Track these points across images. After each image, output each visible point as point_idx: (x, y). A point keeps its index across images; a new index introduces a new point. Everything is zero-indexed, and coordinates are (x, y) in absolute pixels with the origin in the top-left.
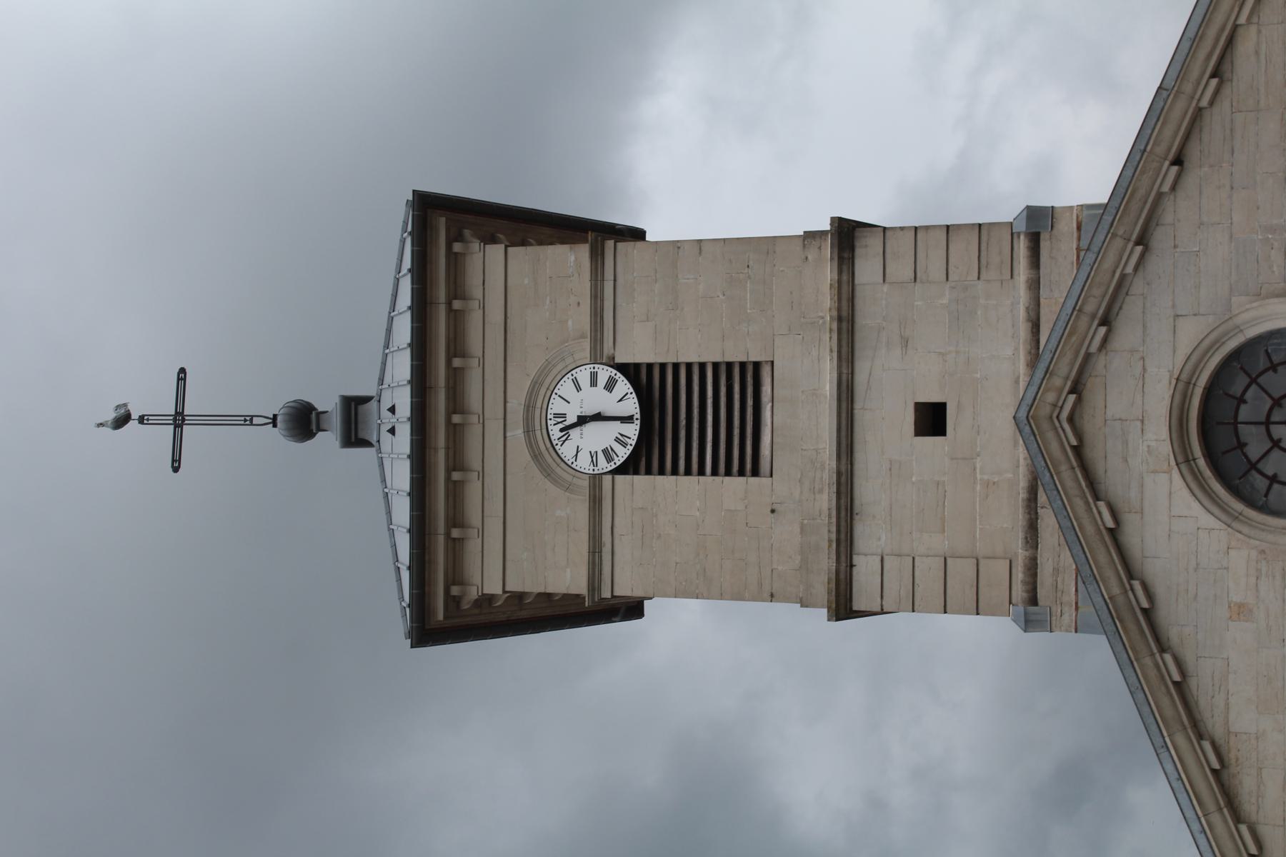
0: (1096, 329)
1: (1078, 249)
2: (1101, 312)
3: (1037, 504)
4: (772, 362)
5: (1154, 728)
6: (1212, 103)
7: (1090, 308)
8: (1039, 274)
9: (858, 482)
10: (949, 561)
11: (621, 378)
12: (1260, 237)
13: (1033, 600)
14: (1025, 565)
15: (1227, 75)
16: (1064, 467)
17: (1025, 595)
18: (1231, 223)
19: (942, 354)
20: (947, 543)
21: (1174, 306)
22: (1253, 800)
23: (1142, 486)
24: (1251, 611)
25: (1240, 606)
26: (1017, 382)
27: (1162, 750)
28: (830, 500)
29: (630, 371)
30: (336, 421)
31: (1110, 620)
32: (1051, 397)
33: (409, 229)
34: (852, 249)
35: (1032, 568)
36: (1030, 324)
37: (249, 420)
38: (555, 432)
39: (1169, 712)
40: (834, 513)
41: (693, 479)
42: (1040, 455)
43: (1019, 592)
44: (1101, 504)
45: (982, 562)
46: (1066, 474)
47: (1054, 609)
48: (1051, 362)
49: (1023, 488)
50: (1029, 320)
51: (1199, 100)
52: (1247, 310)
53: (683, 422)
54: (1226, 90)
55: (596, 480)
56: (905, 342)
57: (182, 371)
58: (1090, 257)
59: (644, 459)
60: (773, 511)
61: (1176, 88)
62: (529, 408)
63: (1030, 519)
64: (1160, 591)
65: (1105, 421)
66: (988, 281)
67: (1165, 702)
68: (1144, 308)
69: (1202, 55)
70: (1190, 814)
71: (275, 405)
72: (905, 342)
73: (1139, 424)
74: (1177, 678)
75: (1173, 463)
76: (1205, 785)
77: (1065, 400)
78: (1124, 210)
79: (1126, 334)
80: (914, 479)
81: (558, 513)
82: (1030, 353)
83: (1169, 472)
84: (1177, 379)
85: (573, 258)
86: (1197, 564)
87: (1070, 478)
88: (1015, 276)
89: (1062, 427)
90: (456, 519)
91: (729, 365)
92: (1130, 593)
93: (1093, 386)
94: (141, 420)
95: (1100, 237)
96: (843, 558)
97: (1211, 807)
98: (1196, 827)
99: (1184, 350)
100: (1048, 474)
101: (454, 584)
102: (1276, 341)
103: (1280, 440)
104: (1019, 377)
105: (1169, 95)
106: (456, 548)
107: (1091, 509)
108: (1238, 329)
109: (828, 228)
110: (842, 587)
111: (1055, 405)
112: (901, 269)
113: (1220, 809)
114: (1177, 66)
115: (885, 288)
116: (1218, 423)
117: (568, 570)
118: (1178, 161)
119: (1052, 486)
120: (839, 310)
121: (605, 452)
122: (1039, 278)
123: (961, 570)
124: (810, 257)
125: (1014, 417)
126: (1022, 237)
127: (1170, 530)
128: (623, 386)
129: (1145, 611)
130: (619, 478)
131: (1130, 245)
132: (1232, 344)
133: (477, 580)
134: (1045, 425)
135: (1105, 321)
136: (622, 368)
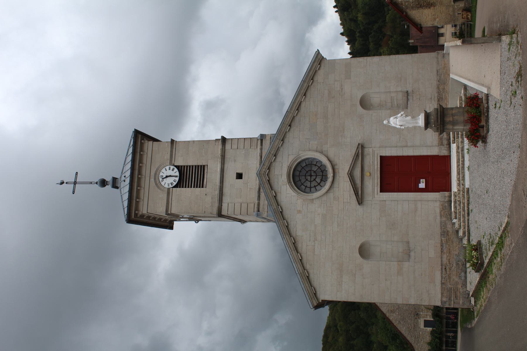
1: (270, 142)
2: (274, 153)
4: (207, 165)
6: (296, 115)
7: (272, 153)
9: (224, 188)
10: (242, 204)
11: (175, 168)
13: (259, 211)
16: (266, 184)
17: (257, 210)
19: (242, 163)
21: (288, 153)
22: (301, 249)
26: (257, 168)
28: (218, 192)
29: (177, 167)
30: (111, 183)
32: (264, 170)
33: (133, 137)
34: (225, 142)
35: (259, 205)
37: (91, 183)
38: (161, 179)
39: (285, 231)
40: (219, 194)
41: (190, 188)
43: (256, 209)
46: (266, 185)
50: (260, 156)
51: (294, 114)
53: (188, 177)
54: (299, 113)
55: (169, 189)
56: (235, 161)
57: (77, 173)
58: (273, 143)
59: (179, 185)
60: (206, 195)
62: (155, 174)
63: (259, 195)
66: (252, 149)
67: (284, 229)
69: (295, 106)
70: (288, 251)
71: (97, 180)
72: (235, 161)
73: (281, 176)
74: (287, 225)
75: (287, 182)
76: (292, 246)
79: (279, 159)
80: (235, 188)
81: (160, 196)
83: (286, 185)
85: (167, 144)
87: (267, 186)
90: (138, 197)
91: (198, 166)
93: (272, 168)
94: (67, 183)
95: (275, 139)
96: (220, 204)
97: (293, 250)
98: (289, 253)
99: (290, 160)
101: (136, 211)
103: (307, 179)
106: (137, 203)
107: (271, 192)
109: (220, 138)
110: (220, 209)
111: (265, 172)
112: (234, 146)
113: (294, 250)
114: (290, 107)
115: (231, 150)
117: (161, 208)
118: (290, 126)
120: (222, 154)
121: (171, 183)
123: (244, 206)
124: (216, 144)
128: (176, 170)
130: (173, 188)
131: (280, 141)
132: (299, 160)
133: (141, 210)
135: (275, 156)
136: (176, 166)
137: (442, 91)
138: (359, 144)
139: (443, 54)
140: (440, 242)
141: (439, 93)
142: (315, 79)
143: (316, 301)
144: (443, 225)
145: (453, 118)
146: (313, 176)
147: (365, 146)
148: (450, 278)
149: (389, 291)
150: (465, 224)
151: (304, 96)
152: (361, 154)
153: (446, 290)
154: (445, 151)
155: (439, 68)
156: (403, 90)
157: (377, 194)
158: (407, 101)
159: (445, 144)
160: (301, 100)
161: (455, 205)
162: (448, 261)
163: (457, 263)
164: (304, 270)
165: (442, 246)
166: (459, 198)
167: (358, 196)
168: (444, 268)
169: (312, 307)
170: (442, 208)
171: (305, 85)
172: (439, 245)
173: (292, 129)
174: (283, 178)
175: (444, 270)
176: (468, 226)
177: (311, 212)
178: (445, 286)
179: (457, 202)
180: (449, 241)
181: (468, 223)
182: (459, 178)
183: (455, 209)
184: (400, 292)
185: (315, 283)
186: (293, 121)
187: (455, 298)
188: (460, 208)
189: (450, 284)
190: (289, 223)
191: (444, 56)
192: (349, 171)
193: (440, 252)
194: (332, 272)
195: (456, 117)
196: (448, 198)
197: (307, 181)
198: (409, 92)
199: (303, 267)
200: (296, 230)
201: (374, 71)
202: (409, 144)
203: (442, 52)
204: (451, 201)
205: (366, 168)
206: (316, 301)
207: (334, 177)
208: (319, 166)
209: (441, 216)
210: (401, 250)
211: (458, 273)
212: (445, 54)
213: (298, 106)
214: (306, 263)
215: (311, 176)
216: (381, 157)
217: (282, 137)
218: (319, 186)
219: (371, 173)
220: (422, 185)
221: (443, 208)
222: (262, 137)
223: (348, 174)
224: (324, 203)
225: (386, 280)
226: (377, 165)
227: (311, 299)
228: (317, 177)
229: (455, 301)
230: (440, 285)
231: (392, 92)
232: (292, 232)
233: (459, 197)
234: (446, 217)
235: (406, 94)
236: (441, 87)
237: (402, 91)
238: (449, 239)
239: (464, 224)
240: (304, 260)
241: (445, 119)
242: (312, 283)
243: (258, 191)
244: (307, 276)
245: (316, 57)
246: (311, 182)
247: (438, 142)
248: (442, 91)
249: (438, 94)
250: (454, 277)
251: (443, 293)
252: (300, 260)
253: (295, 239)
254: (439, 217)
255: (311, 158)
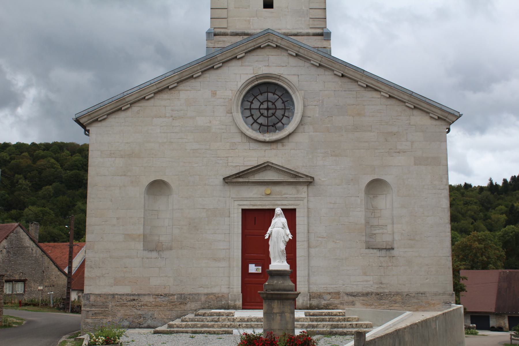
0: (295, 53)
1: (318, 47)
2: (300, 54)
3: (243, 35)
5: (180, 70)
6: (359, 85)
7: (301, 50)
8: (311, 36)
10: (226, 10)
12: (320, 99)
13: (215, 35)
14: (225, 32)
15: (367, 89)
16: (254, 43)
17: (217, 32)
18: (325, 91)
20: (232, 9)
21: (301, 75)
22: (161, 98)
23: (249, 66)
24: (214, 97)
25: (216, 94)
26: (279, 29)
27: (173, 72)
31: (210, 57)
32: (275, 39)
35: (225, 34)
36: (296, 33)
39: (184, 74)
42: (258, 36)
43: (218, 31)
44: (244, 54)
45: (226, 19)
46: (252, 44)
47: (213, 41)
48: (285, 39)
49: (248, 31)
50: (298, 33)
51: (360, 82)
52: (300, 95)
54: (362, 89)
58: (316, 51)
61: (364, 75)
64: (219, 71)
65: (268, 55)
66: (309, 21)
67: (187, 73)
68: (301, 66)
69: (373, 82)
70: (156, 80)
73: (267, 65)
74: (194, 76)
75: (256, 75)
76: (164, 84)
77: (274, 44)
78: (329, 60)
79: (293, 61)
82: (288, 33)
84: (280, 76)
86: (227, 82)
87: (251, 45)
88: (311, 29)
89: (266, 43)
92: (218, 63)
93: (278, 52)
95: (321, 54)
97: (158, 86)
98: (152, 82)
99: (289, 78)
100: (252, 39)
102: (291, 103)
103: (263, 104)
104: (281, 30)
105: (362, 73)
107: (242, 51)
108: (294, 93)
111: (272, 41)
113: (157, 89)
116: (267, 87)
118: (343, 76)
119: (249, 40)
122: (310, 36)
123: (224, 13)
125: (269, 29)
126: (322, 31)
127: (237, 74)
129: (213, 67)
131: (319, 62)
132: (290, 91)
134: (267, 38)
135: (297, 55)
137: (393, 298)
138: (313, 178)
139: (450, 303)
140: (171, 293)
141: (390, 294)
142: (416, 112)
143: (86, 122)
144: (194, 297)
145: (277, 313)
146: (268, 112)
147: (311, 188)
148: (122, 305)
149: (103, 223)
150: (183, 328)
151: (388, 96)
152: (297, 180)
153: (104, 300)
154: (301, 302)
155: (428, 295)
156: (395, 242)
157: (240, 205)
158: (378, 249)
159: (311, 302)
160: (383, 91)
161: (215, 315)
162: (144, 304)
163: (142, 316)
164: (131, 104)
165: (166, 295)
166: (222, 320)
167: (236, 178)
168: (135, 299)
169: (77, 116)
170: (218, 297)
171: (406, 97)
172: (167, 291)
173: (337, 79)
174: (264, 68)
175: (132, 297)
176: (177, 332)
177: (214, 111)
178: (110, 298)
179: (218, 317)
180: (173, 305)
181: (182, 332)
182: (252, 321)
183: (209, 314)
184: (102, 238)
185: (112, 120)
186: (352, 81)
187: (93, 312)
188: (208, 321)
189: (112, 307)
190: (197, 80)
191: (446, 303)
192: (272, 163)
193: (157, 293)
194: (128, 143)
195: (278, 317)
196: (233, 305)
197: (259, 103)
198: (392, 251)
199: (135, 102)
200: (187, 90)
201: (426, 200)
202: (312, 251)
203: (452, 300)
204: (228, 309)
205: (277, 189)
206: (86, 122)
207: (264, 142)
208: (282, 121)
209: (207, 294)
210: (162, 239)
211: (129, 317)
212: (450, 305)
213: (373, 87)
214: (141, 106)
215: (268, 109)
216: (294, 210)
217: (326, 65)
218: (252, 121)
219: (271, 196)
220: (253, 269)
221: (218, 297)
222: (326, 35)
223: (268, 162)
224: (226, 129)
225: (118, 219)
226: (290, 205)
227: (89, 114)
228: (266, 119)
229: (90, 312)
230: (111, 293)
231: (393, 226)
232: (184, 84)
233: (224, 320)
234: (206, 301)
235: (390, 247)
236: (398, 298)
237: (393, 240)
238: (175, 305)
239: (183, 326)
240: (143, 104)
241: (276, 301)
242: (113, 116)
243: (245, 33)
244: (121, 108)
245: (450, 113)
246: (258, 110)
247: (315, 291)
248: (392, 299)
249: (388, 293)
250: (122, 311)
251: (101, 296)
252: (145, 98)
253: (174, 89)
254: (206, 291)
255: (294, 109)
